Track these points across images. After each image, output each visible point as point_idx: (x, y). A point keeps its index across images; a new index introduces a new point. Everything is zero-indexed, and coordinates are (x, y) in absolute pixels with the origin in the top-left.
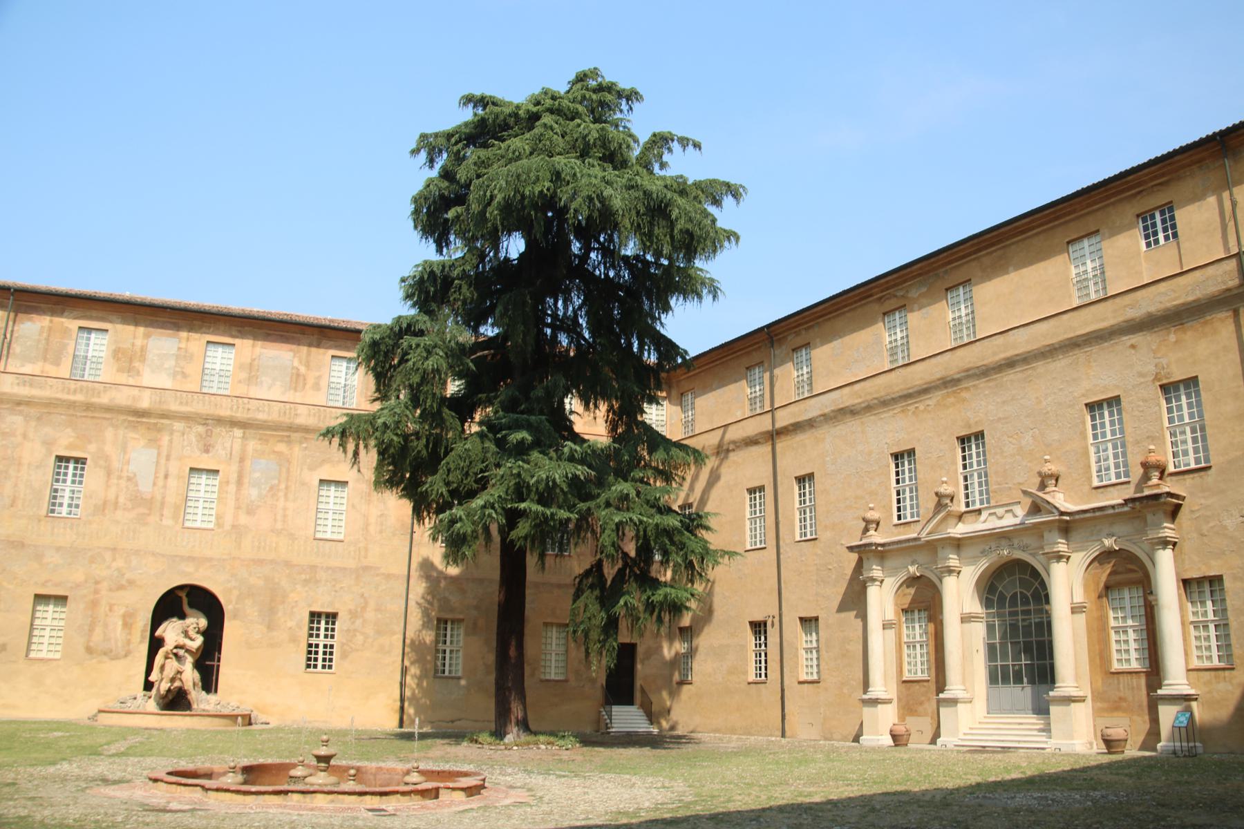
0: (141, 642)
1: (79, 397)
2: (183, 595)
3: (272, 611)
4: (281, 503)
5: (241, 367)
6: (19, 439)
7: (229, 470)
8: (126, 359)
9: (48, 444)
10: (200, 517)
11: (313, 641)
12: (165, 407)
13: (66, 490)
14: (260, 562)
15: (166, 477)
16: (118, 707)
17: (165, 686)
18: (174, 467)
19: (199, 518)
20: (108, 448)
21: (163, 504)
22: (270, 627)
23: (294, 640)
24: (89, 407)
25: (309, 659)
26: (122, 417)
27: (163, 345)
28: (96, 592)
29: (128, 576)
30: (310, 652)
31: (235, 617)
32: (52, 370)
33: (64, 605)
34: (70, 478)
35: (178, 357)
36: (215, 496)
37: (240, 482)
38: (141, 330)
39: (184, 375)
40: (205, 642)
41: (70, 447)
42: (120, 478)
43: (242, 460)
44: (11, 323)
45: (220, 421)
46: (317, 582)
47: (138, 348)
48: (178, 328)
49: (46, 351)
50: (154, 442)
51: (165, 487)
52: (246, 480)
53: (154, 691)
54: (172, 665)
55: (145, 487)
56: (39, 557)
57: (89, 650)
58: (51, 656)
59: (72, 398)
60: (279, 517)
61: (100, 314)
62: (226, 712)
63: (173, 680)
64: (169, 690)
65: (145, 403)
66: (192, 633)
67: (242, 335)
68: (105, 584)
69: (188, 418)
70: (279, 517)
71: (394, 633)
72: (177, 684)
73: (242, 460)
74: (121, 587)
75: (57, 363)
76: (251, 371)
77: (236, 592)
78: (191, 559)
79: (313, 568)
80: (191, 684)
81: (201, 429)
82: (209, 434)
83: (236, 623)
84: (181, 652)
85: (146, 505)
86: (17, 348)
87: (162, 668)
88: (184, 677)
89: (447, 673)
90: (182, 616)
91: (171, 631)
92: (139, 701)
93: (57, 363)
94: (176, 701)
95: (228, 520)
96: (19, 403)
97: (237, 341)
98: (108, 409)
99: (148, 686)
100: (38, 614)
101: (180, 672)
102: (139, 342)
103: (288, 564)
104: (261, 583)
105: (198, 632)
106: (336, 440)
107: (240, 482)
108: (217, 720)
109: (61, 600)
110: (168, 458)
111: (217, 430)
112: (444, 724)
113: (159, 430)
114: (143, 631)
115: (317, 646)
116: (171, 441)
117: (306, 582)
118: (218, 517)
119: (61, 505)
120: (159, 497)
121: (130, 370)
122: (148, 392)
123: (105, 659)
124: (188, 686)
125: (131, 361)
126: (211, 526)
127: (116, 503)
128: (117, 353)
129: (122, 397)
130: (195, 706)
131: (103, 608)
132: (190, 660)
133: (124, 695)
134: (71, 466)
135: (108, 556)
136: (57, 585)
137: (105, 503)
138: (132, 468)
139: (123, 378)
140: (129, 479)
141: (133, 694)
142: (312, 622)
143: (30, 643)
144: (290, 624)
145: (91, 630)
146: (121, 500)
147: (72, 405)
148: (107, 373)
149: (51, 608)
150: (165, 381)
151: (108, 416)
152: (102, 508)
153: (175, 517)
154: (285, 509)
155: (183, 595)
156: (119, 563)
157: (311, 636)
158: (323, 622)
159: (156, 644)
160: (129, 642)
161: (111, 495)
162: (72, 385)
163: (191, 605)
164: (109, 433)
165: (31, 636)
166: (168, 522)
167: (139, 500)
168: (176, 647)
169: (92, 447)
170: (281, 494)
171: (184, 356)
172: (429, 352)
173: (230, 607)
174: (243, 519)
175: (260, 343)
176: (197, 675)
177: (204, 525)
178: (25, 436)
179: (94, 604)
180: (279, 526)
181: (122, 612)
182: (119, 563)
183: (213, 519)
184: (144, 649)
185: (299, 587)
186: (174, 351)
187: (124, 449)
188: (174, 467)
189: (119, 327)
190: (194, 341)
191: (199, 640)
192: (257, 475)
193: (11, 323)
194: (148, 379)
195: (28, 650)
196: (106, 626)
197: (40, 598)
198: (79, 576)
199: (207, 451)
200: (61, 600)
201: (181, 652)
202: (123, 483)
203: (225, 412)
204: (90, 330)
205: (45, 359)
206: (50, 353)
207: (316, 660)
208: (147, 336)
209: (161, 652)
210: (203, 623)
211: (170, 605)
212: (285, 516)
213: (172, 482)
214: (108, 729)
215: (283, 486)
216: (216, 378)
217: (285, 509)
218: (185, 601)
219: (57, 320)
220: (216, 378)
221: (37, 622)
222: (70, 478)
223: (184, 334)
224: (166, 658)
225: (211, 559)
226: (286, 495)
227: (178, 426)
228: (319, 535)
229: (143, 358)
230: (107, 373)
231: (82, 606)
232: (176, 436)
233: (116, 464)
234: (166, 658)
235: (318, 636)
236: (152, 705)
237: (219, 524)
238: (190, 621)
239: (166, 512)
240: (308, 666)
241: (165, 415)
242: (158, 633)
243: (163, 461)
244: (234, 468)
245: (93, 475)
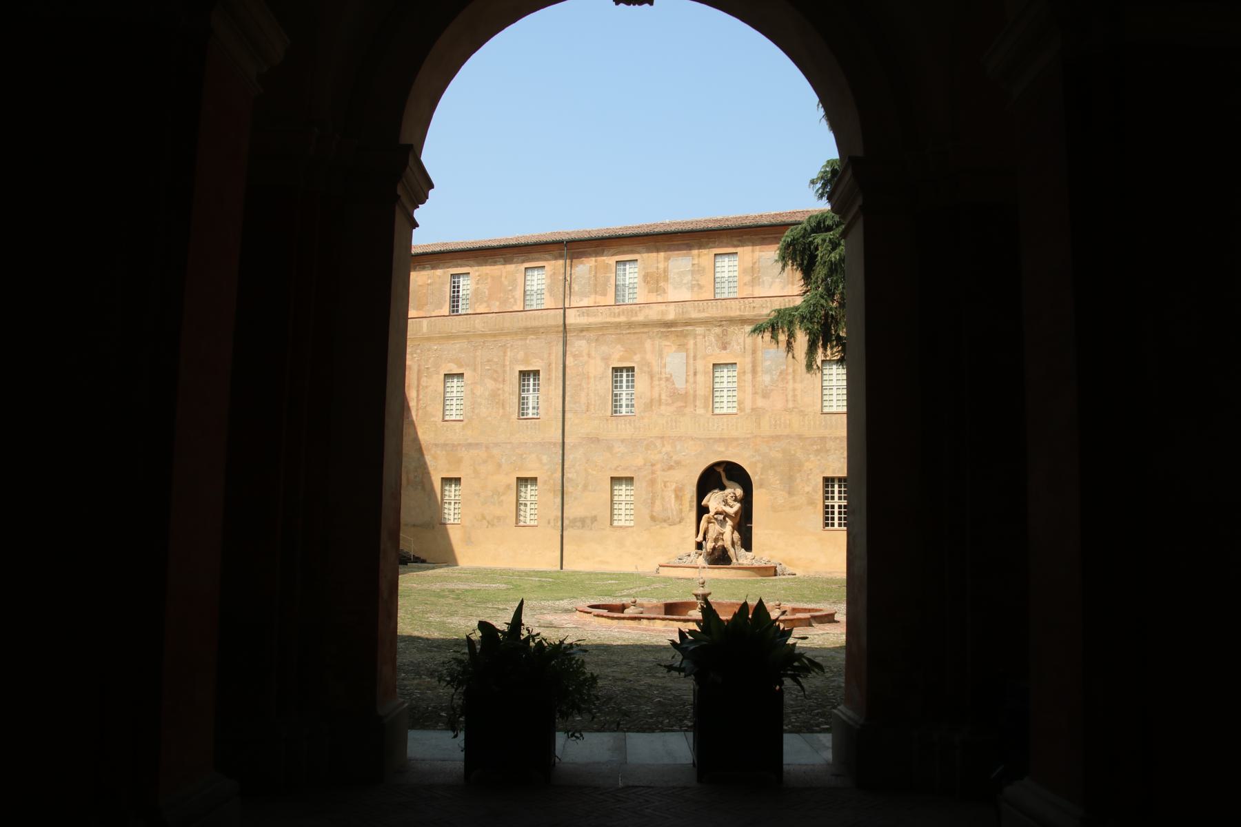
1: (622, 319)
2: (720, 470)
3: (791, 478)
4: (790, 385)
5: (744, 271)
6: (586, 358)
7: (745, 362)
8: (654, 281)
9: (606, 359)
10: (725, 405)
11: (829, 503)
12: (687, 316)
13: (624, 394)
14: (777, 438)
15: (695, 374)
16: (677, 562)
18: (700, 365)
19: (725, 405)
20: (649, 357)
21: (695, 396)
22: (790, 493)
23: (811, 502)
24: (630, 325)
25: (827, 519)
26: (656, 330)
27: (680, 263)
28: (653, 473)
29: (675, 458)
30: (827, 513)
31: (761, 486)
32: (602, 300)
33: (632, 485)
34: (624, 384)
35: (693, 272)
36: (735, 385)
37: (754, 372)
38: (662, 254)
39: (700, 287)
40: (741, 508)
41: (620, 360)
42: (660, 379)
43: (754, 352)
44: (568, 268)
45: (732, 321)
46: (827, 451)
47: (661, 270)
48: (689, 247)
49: (595, 285)
50: (682, 347)
51: (695, 382)
52: (759, 369)
54: (714, 529)
55: (680, 384)
56: (610, 448)
57: (653, 518)
58: (628, 524)
59: (617, 320)
60: (790, 397)
61: (630, 248)
62: (756, 565)
63: (716, 540)
64: (714, 549)
65: (671, 316)
66: (730, 501)
67: (742, 243)
68: (659, 466)
69: (705, 322)
70: (790, 397)
72: (720, 543)
73: (754, 352)
74: (670, 468)
75: (604, 294)
76: (754, 274)
77: (760, 465)
78: (721, 440)
79: (823, 439)
81: (718, 330)
82: (725, 333)
83: (764, 490)
85: (682, 399)
86: (575, 287)
90: (723, 488)
91: (714, 501)
93: (604, 294)
94: (720, 558)
95: (748, 405)
96: (582, 331)
97: (739, 250)
98: (645, 325)
99: (699, 546)
100: (616, 492)
102: (661, 266)
103: (800, 437)
104: (780, 455)
105: (735, 500)
106: (767, 335)
107: (754, 372)
108: (741, 572)
109: (629, 480)
110: (695, 358)
111: (731, 329)
113: (685, 336)
114: (691, 501)
115: (833, 507)
116: (695, 344)
117: (818, 452)
118: (740, 403)
119: (621, 406)
120: (692, 392)
121: (657, 290)
122: (672, 306)
123: (665, 525)
124: (728, 544)
125: (657, 282)
126: (735, 411)
127: (660, 400)
128: (647, 278)
129: (653, 314)
130: (734, 561)
131: (659, 485)
132: (729, 523)
133: (682, 553)
134: (625, 374)
135: (658, 443)
136: (625, 469)
137: (652, 400)
138: (668, 370)
139: (653, 298)
140: (667, 379)
142: (827, 486)
143: (612, 515)
144: (807, 489)
145: (653, 503)
146: (663, 397)
147: (618, 326)
148: (641, 296)
149: (624, 487)
150: (686, 295)
151: (646, 330)
152: (650, 405)
153: (706, 407)
154: (794, 390)
156: (668, 448)
157: (827, 498)
158: (836, 488)
159: (702, 510)
160: (681, 511)
161: (656, 395)
162: (616, 309)
163: (730, 478)
164: (648, 344)
165: (612, 509)
166: (700, 411)
167: (675, 396)
169: (637, 358)
170: (790, 377)
171: (697, 270)
172: (835, 245)
174: (760, 402)
175: (758, 247)
176: (736, 535)
177: (730, 411)
178: (589, 355)
179: (652, 482)
180: (790, 405)
181: (674, 486)
182: (668, 448)
183: (735, 404)
184: (693, 515)
185: (812, 457)
186: (689, 268)
187: (661, 356)
188: (700, 365)
189: (645, 255)
190: (703, 256)
191: (737, 506)
192: (768, 363)
193: (568, 268)
194: (673, 294)
195: (612, 520)
196: (663, 498)
197: (615, 480)
199: (725, 348)
200: (629, 480)
201: (721, 517)
202: (663, 383)
203: (735, 313)
204: (624, 262)
205: (596, 293)
206: (598, 287)
207: (833, 519)
208: (667, 259)
209: (705, 517)
210: (739, 492)
211: (711, 479)
212: (794, 396)
213: (701, 378)
214: (667, 580)
215: (790, 370)
216: (726, 285)
217: (794, 390)
218: (723, 474)
219: (600, 259)
220: (726, 285)
221: (616, 498)
222: (624, 384)
223: (695, 252)
224: (709, 522)
225: (737, 439)
226: (794, 378)
227: (700, 330)
228: (826, 410)
229: (666, 279)
230: (641, 296)
231: (644, 484)
232: (699, 339)
233: (656, 369)
234: (709, 522)
235: (833, 498)
236: (701, 561)
237: (741, 409)
238: (728, 491)
239: (698, 403)
240: (827, 525)
241: (688, 323)
243: (691, 361)
244: (748, 359)
245: (641, 380)
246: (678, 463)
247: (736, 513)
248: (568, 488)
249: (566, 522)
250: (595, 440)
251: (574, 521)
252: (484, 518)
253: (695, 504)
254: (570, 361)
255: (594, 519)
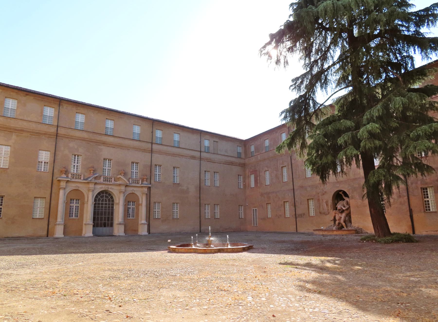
28: (319, 197)
29: (324, 191)
57: (320, 213)
68: (320, 194)
71: (405, 196)
74: (324, 194)
89: (431, 210)
112: (433, 232)
131: (321, 201)
145: (320, 207)
160: (328, 210)
179: (319, 200)
196: (323, 205)
198: (314, 193)
246: (325, 192)
248: (297, 204)
249: (297, 216)
250: (302, 187)
251: (299, 215)
252: (277, 215)
254: (293, 162)
255: (304, 214)
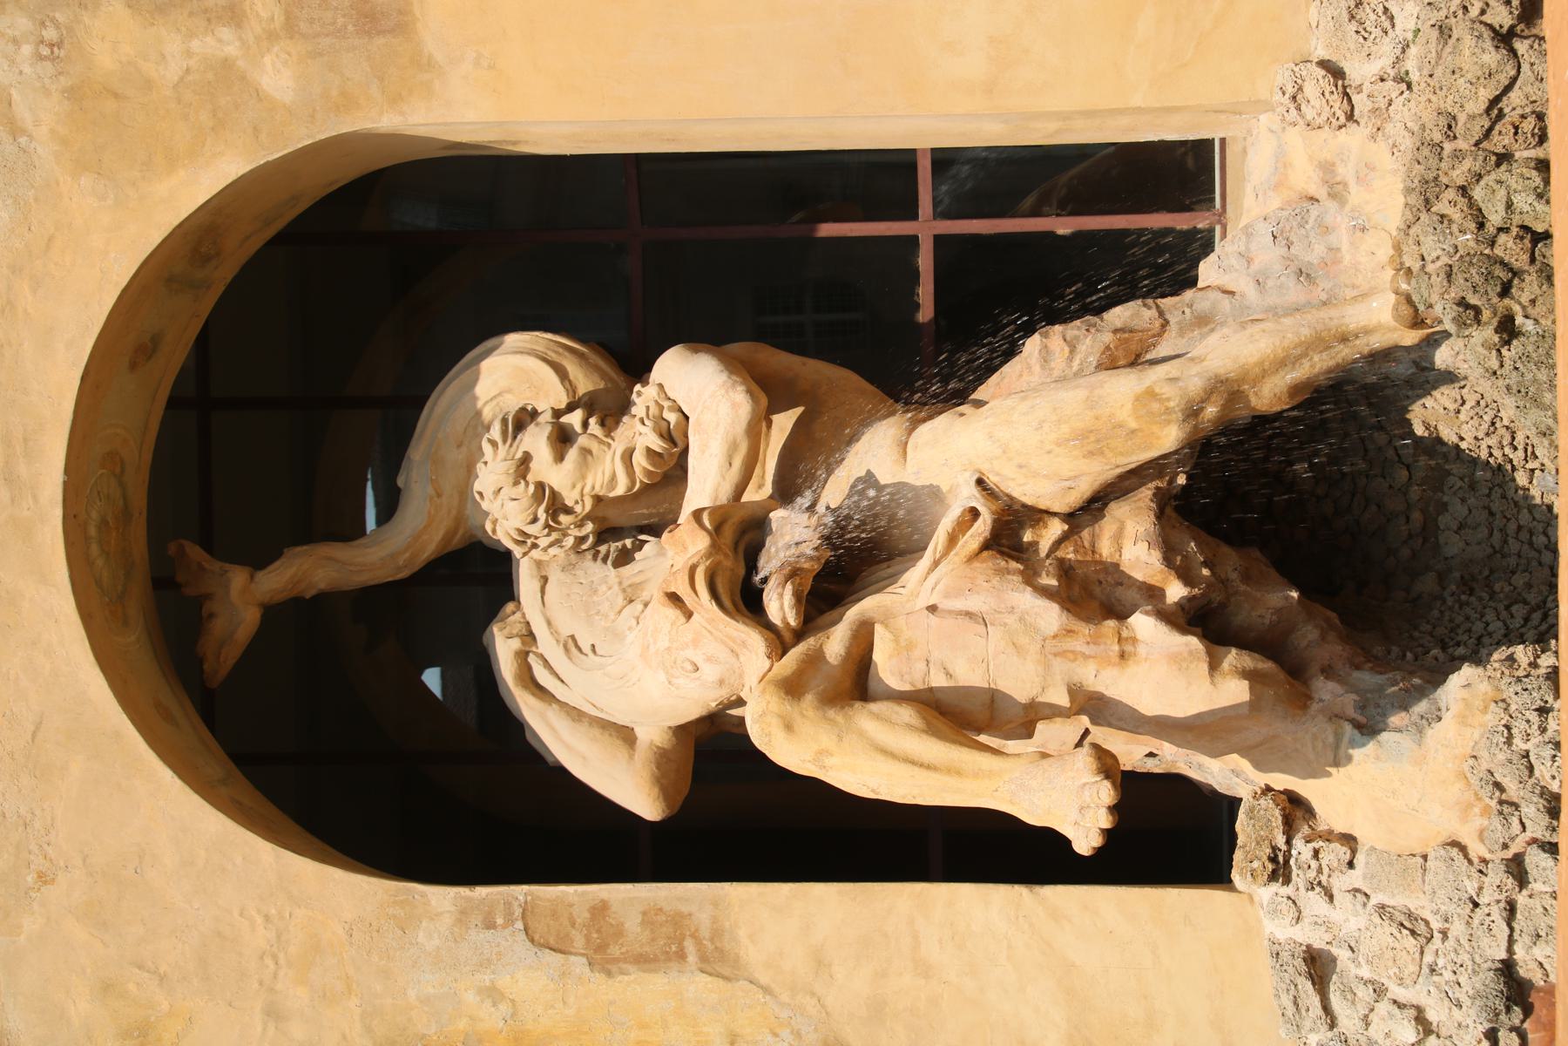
0: (718, 960)
2: (243, 598)
17: (1166, 675)
53: (1222, 772)
63: (1093, 596)
64: (1206, 621)
66: (608, 466)
72: (1132, 543)
80: (1123, 387)
84: (794, 535)
87: (961, 715)
88: (1050, 479)
90: (477, 576)
91: (615, 670)
92: (1338, 921)
99: (1169, 836)
101: (1009, 534)
114: (605, 951)
130: (1377, 319)
141: (1266, 989)
155: (243, 598)
159: (739, 816)
168: (746, 600)
173: (278, 77)
191: (697, 389)
209: (799, 743)
210: (516, 372)
211: (358, 723)
224: (857, 683)
234: (857, 683)
238: (505, 515)
242: (636, 793)
247: (771, 393)
253: (629, 900)
